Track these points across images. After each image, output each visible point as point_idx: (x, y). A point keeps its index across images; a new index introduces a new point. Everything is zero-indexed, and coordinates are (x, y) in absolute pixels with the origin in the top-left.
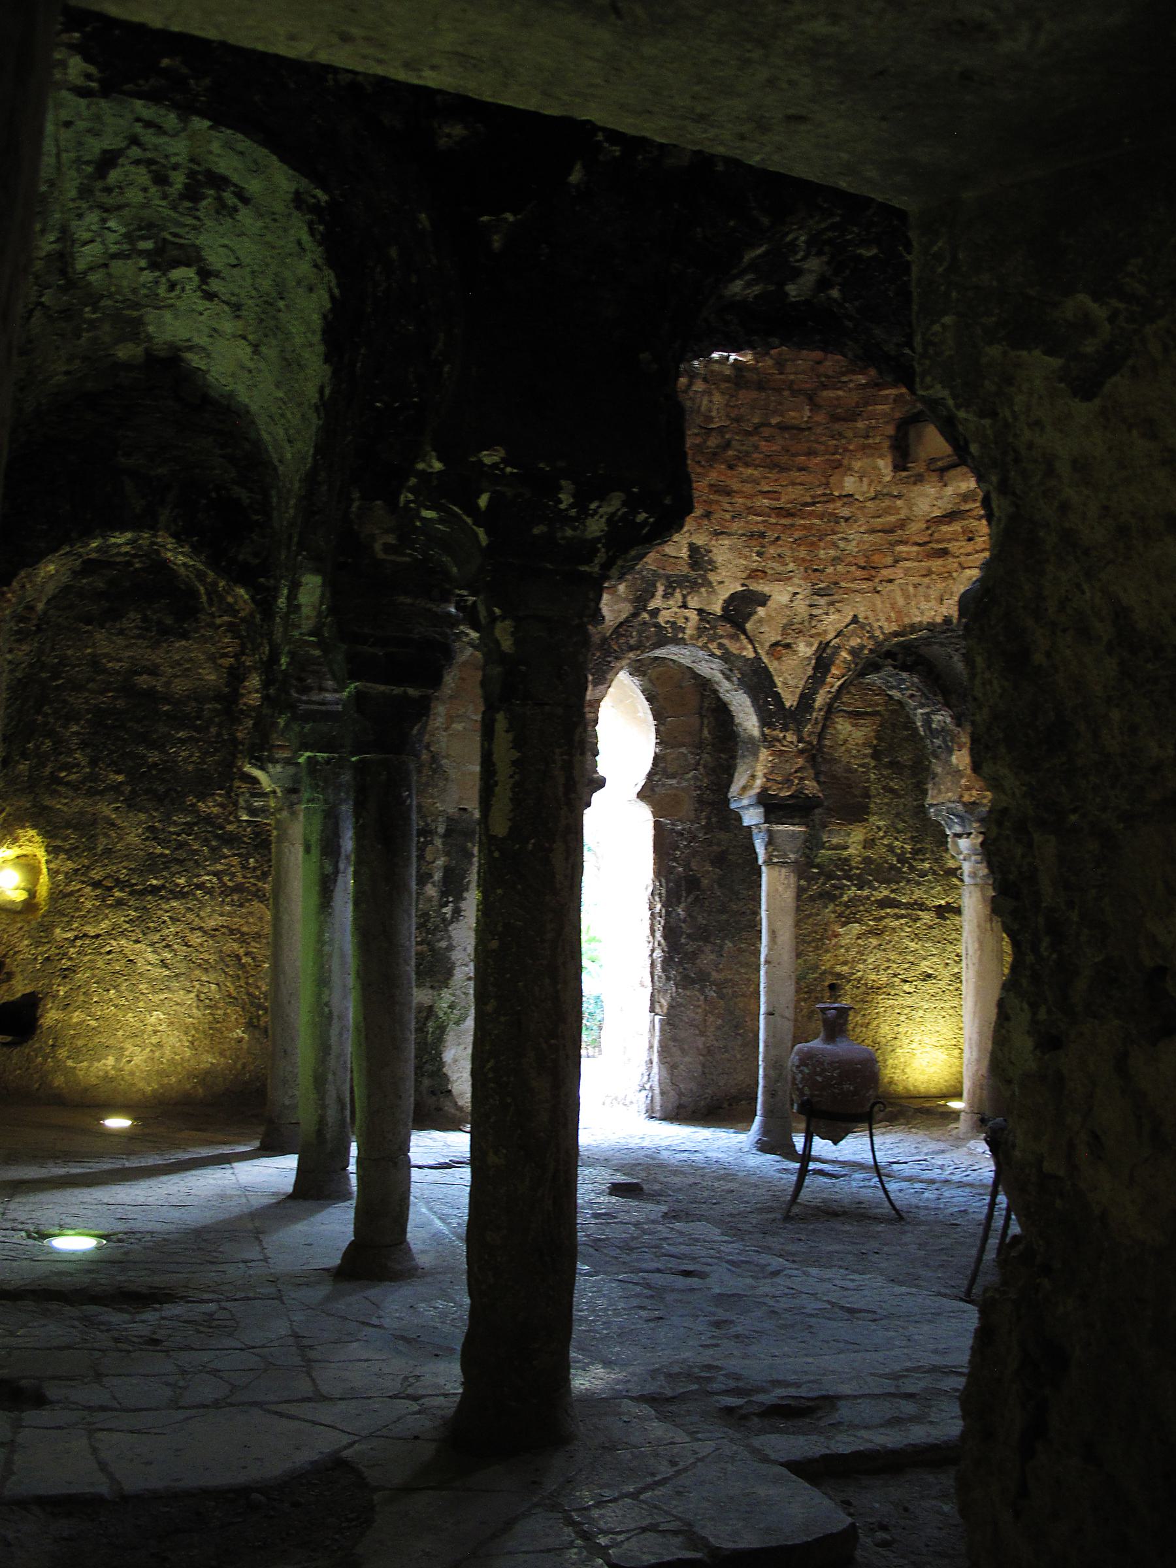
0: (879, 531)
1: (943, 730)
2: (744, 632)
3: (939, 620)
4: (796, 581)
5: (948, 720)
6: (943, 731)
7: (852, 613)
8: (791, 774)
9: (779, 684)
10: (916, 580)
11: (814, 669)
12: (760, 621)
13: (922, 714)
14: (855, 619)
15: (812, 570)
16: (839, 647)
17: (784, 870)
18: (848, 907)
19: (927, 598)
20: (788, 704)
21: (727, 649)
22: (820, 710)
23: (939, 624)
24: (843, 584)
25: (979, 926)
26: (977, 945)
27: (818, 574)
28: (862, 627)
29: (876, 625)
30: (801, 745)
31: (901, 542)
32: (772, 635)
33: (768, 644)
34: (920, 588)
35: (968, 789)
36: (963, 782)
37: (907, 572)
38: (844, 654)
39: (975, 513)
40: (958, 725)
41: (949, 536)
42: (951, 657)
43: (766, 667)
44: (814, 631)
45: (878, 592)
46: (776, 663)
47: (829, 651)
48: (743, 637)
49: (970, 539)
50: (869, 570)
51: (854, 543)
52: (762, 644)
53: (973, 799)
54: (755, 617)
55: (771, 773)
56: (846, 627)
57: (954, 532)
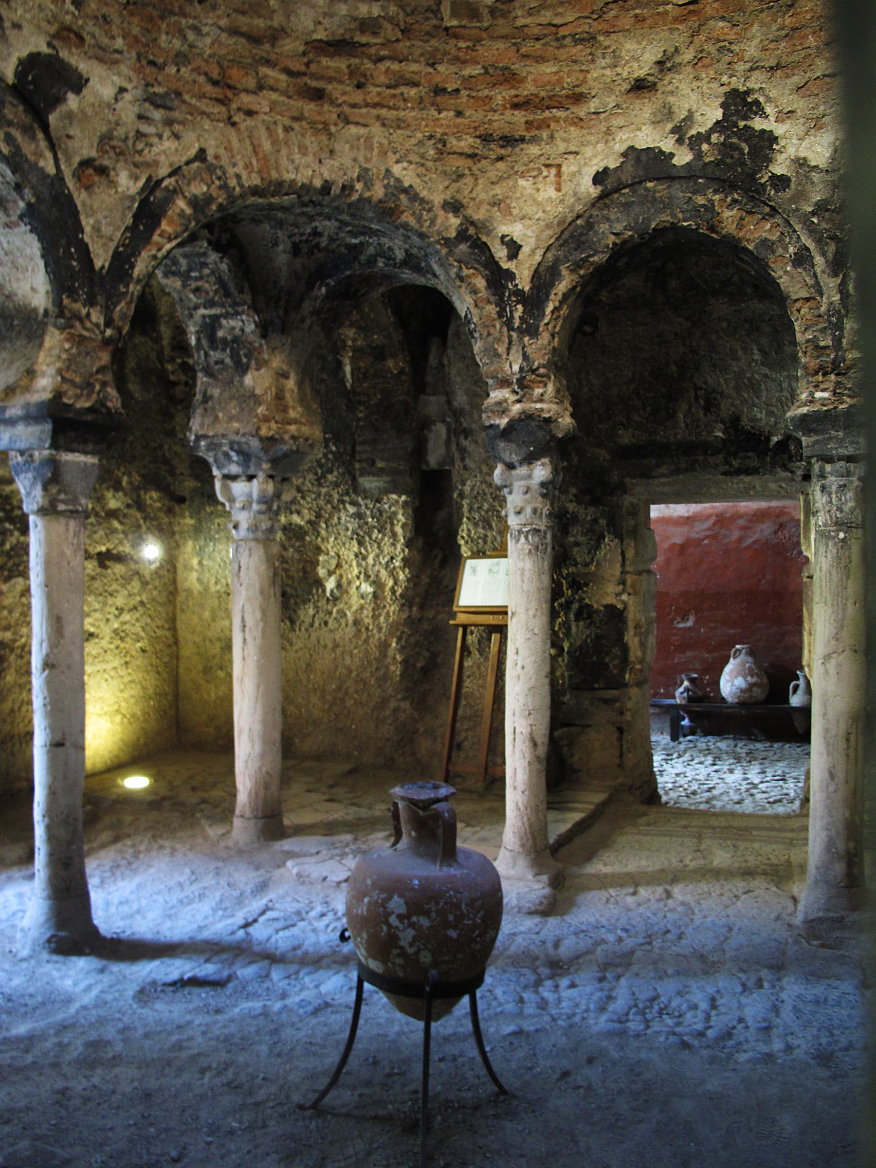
0: (242, 35)
1: (236, 340)
2: (45, 127)
3: (318, 183)
4: (123, 68)
5: (250, 328)
6: (236, 343)
7: (197, 146)
8: (91, 375)
9: (88, 229)
10: (288, 122)
11: (135, 216)
12: (70, 116)
13: (204, 317)
14: (201, 155)
15: (149, 63)
16: (175, 191)
17: (72, 524)
18: (10, 557)
19: (303, 150)
20: (98, 264)
21: (18, 149)
22: (139, 281)
23: (315, 189)
24: (186, 97)
25: (262, 592)
26: (258, 615)
27: (155, 70)
28: (211, 169)
29: (231, 171)
30: (109, 332)
31: (268, 62)
32: (84, 147)
33: (76, 160)
34: (292, 133)
35: (266, 419)
36: (261, 410)
37: (273, 105)
38: (181, 204)
39: (373, 51)
40: (264, 336)
41: (331, 73)
42: (276, 244)
43: (70, 198)
44: (137, 158)
45: (234, 124)
46: (84, 194)
47: (159, 194)
48: (40, 135)
49: (359, 86)
50: (224, 87)
51: (208, 41)
52: (68, 159)
53: (271, 433)
54: (62, 109)
55: (68, 369)
56: (188, 163)
57: (338, 70)
